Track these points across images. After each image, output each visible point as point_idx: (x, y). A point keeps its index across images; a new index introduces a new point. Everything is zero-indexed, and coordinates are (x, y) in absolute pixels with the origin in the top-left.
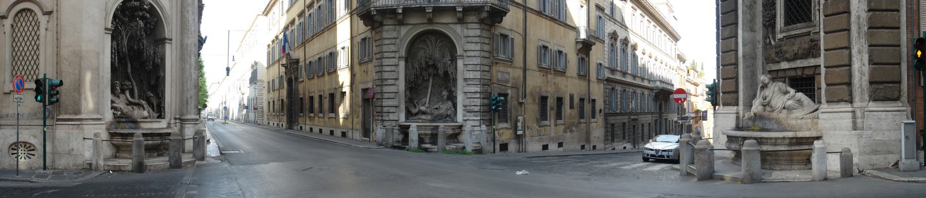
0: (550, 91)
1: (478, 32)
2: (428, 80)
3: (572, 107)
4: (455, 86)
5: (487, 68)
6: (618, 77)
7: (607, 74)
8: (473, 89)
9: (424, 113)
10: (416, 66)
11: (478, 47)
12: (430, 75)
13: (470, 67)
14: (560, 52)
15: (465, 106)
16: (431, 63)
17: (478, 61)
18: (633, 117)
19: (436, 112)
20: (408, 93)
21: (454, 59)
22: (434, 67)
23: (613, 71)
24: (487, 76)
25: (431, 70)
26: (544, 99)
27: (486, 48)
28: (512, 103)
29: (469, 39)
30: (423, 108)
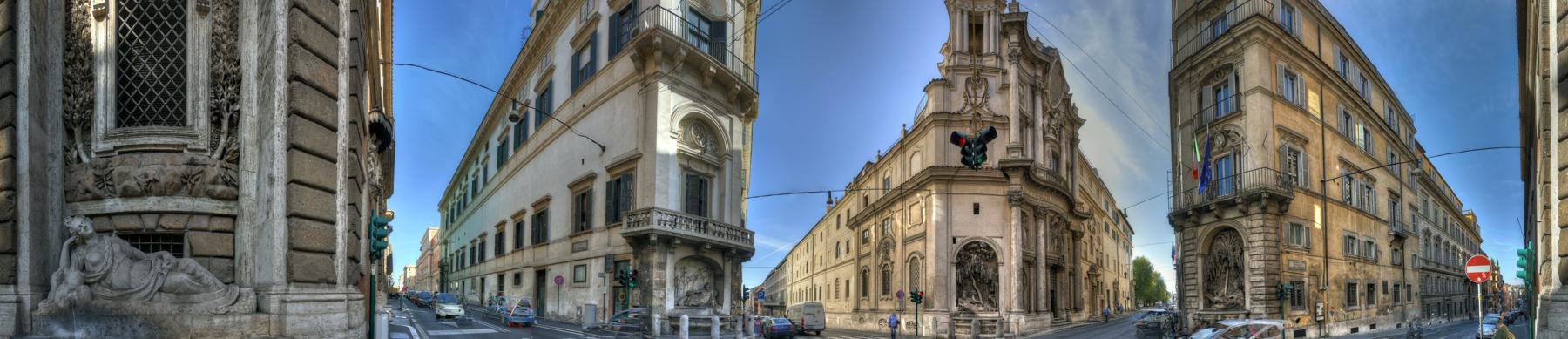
0: (1360, 278)
3: (1385, 292)
6: (1433, 266)
7: (1422, 264)
8: (1258, 278)
14: (1370, 243)
17: (1262, 250)
23: (1427, 262)
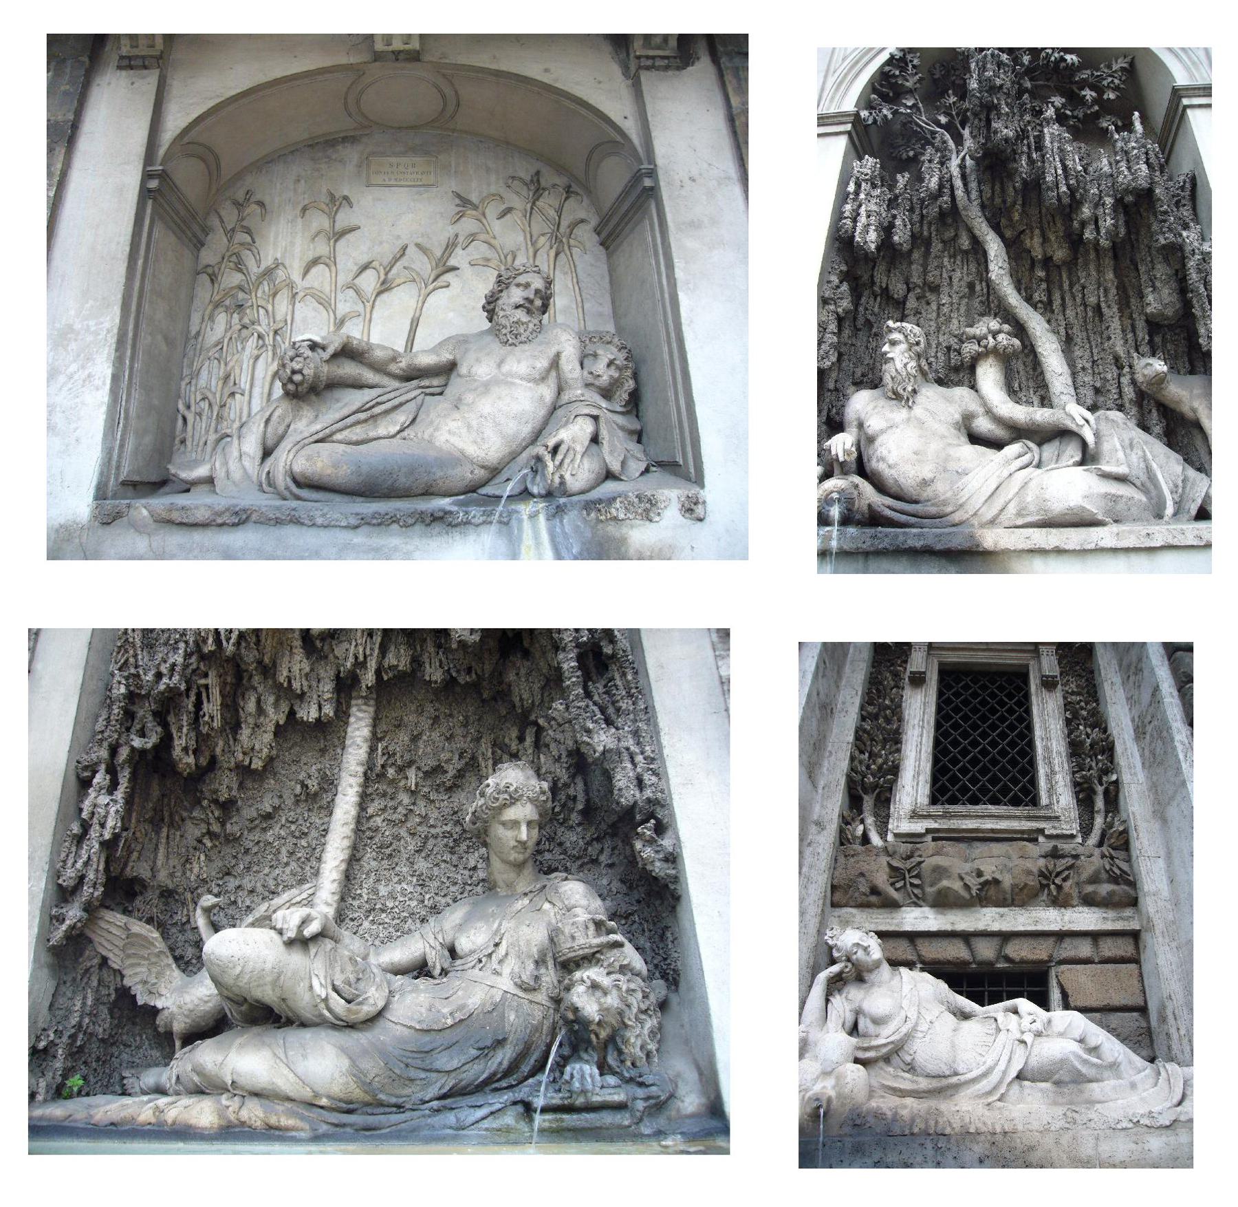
2: (327, 733)
19: (415, 1005)
20: (108, 807)
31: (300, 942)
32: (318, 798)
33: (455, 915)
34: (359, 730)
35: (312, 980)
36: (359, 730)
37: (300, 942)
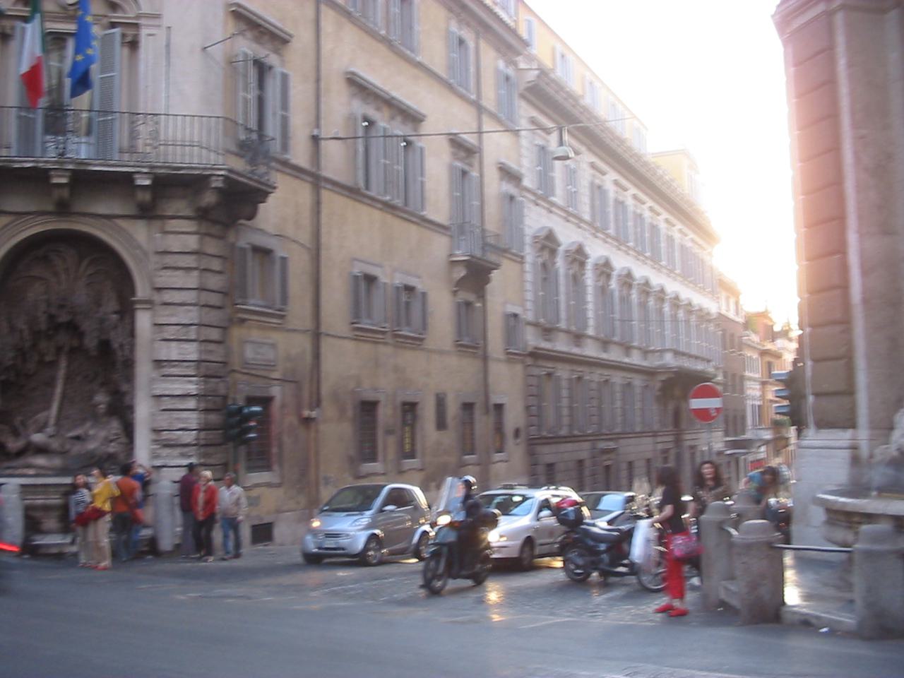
0: (384, 388)
1: (192, 242)
2: (53, 364)
3: (441, 424)
4: (130, 378)
5: (215, 334)
6: (561, 345)
7: (532, 339)
8: (178, 387)
9: (42, 450)
10: (21, 324)
11: (192, 280)
12: (59, 350)
13: (170, 332)
14: (409, 289)
15: (157, 431)
16: (63, 318)
17: (190, 315)
18: (602, 445)
19: (77, 448)
21: (127, 310)
22: (73, 328)
23: (548, 331)
24: (217, 354)
25: (63, 338)
26: (368, 408)
27: (214, 282)
28: (283, 419)
29: (169, 260)
30: (37, 438)
31: (51, 437)
32: (51, 383)
33: (88, 424)
34: (63, 364)
35: (55, 444)
36: (63, 364)
37: (51, 437)
